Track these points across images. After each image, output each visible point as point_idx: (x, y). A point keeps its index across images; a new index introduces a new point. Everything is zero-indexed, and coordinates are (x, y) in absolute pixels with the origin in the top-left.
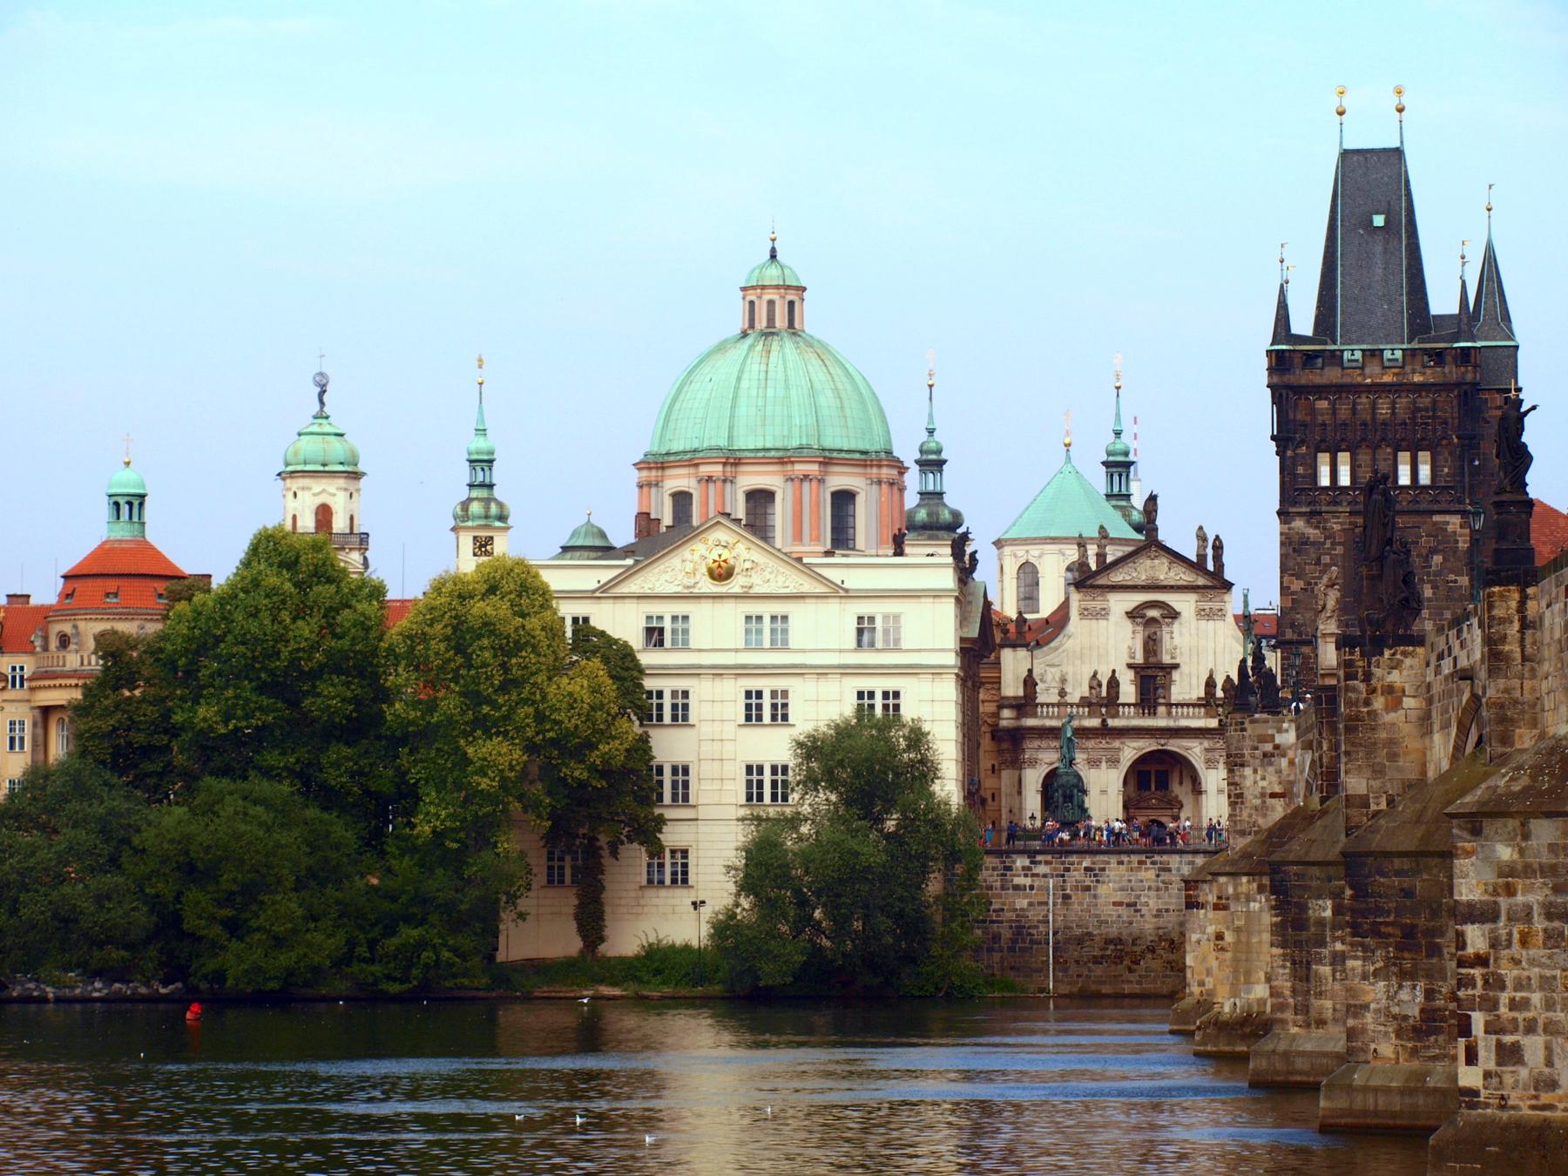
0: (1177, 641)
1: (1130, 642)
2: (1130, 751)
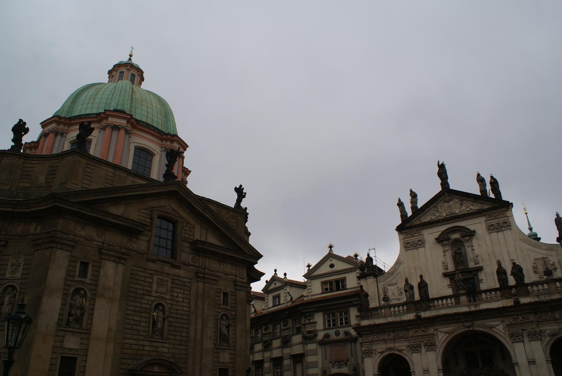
0: (477, 251)
1: (443, 259)
2: (442, 336)
